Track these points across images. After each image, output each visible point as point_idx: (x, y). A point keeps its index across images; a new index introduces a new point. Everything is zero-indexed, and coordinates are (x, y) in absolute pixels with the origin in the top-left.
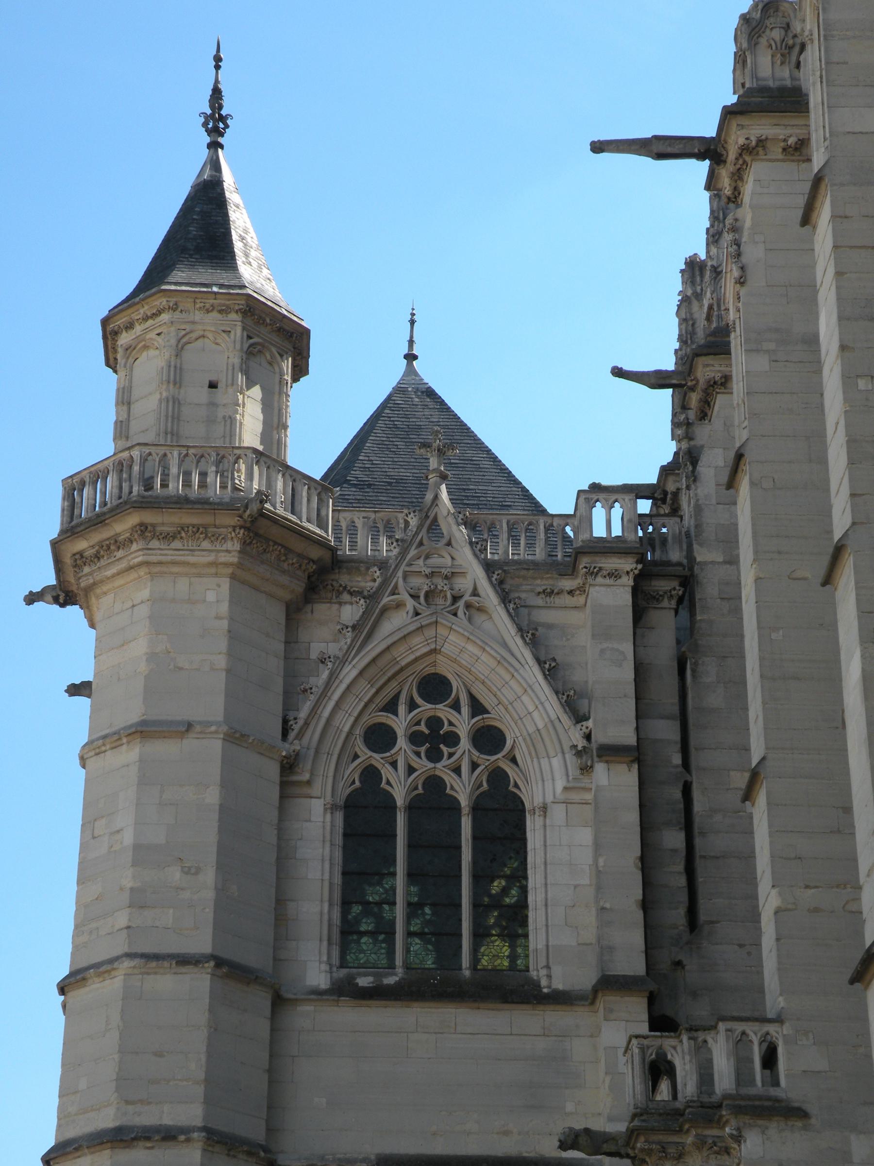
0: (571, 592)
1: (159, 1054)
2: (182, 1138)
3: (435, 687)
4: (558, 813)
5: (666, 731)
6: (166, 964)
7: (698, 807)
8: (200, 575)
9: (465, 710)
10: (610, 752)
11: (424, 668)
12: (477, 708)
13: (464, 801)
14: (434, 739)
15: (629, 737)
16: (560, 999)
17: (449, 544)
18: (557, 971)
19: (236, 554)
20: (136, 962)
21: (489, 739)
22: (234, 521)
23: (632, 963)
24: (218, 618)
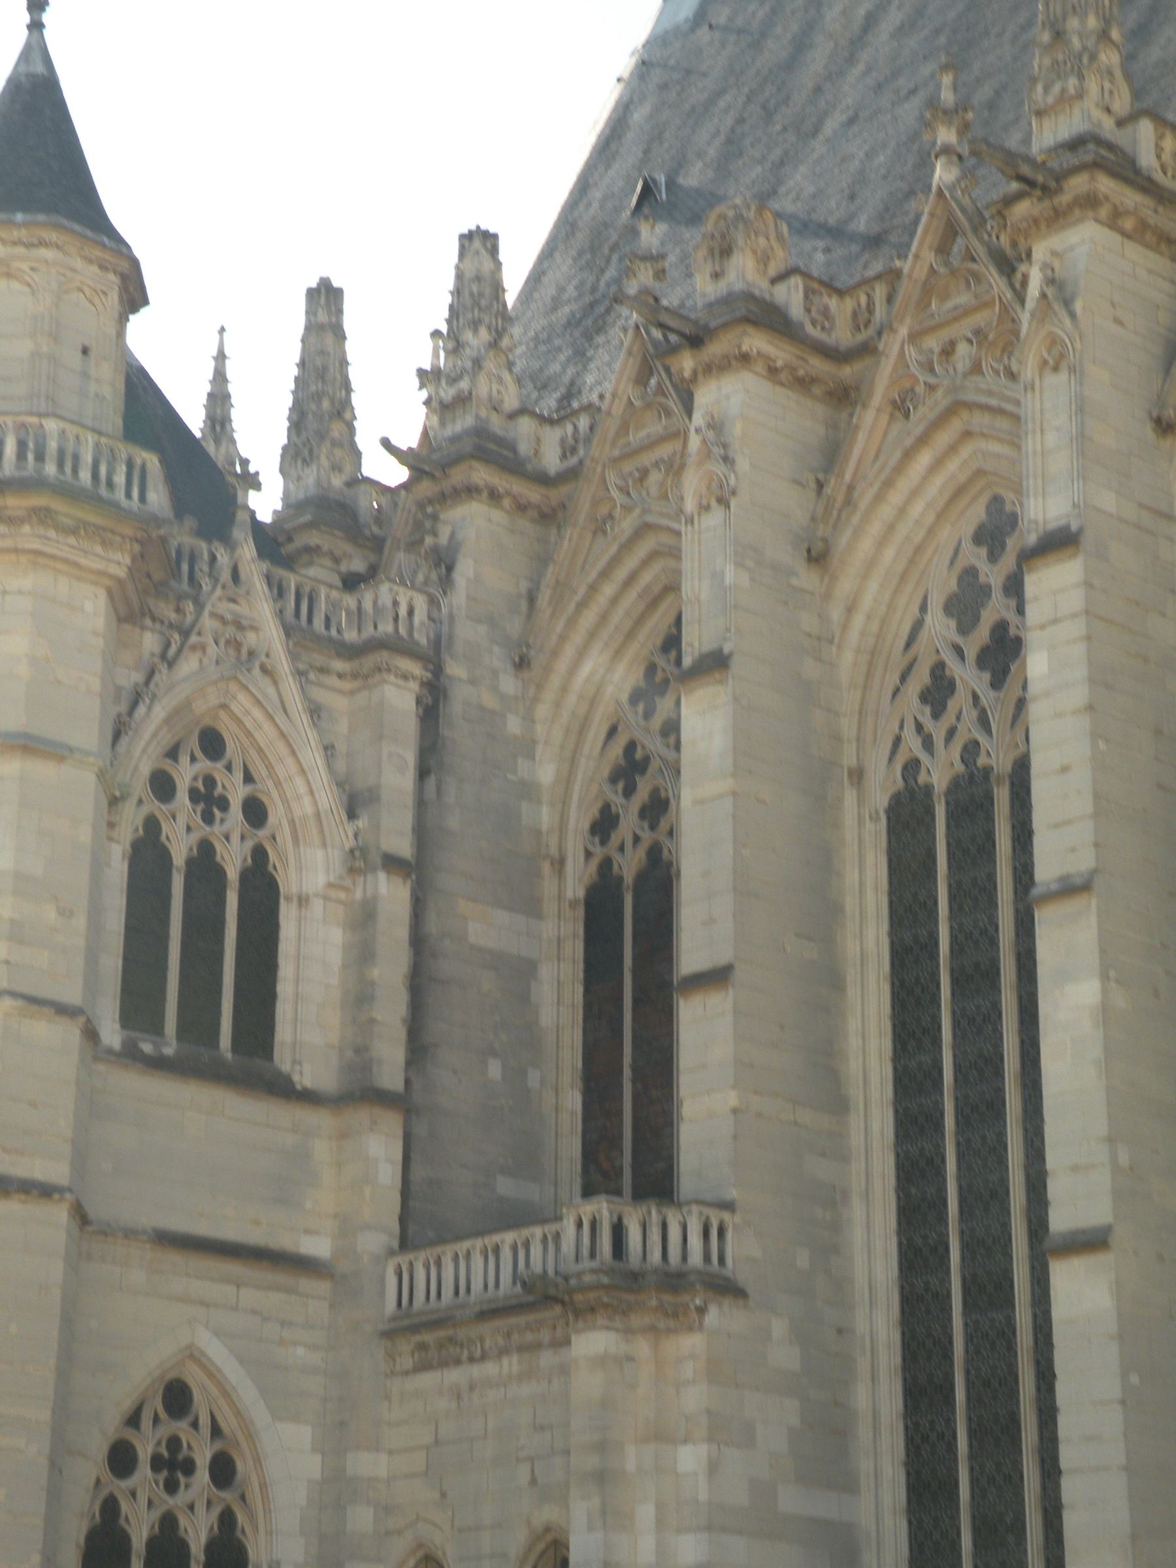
0: (340, 676)
1: (33, 1105)
2: (56, 1196)
3: (212, 744)
4: (317, 906)
6: (46, 1010)
8: (79, 579)
9: (239, 776)
11: (207, 721)
12: (248, 778)
13: (233, 874)
14: (209, 800)
16: (309, 1097)
17: (248, 593)
18: (307, 1068)
19: (125, 569)
20: (20, 1003)
21: (255, 812)
22: (129, 531)
23: (391, 1077)
24: (95, 633)
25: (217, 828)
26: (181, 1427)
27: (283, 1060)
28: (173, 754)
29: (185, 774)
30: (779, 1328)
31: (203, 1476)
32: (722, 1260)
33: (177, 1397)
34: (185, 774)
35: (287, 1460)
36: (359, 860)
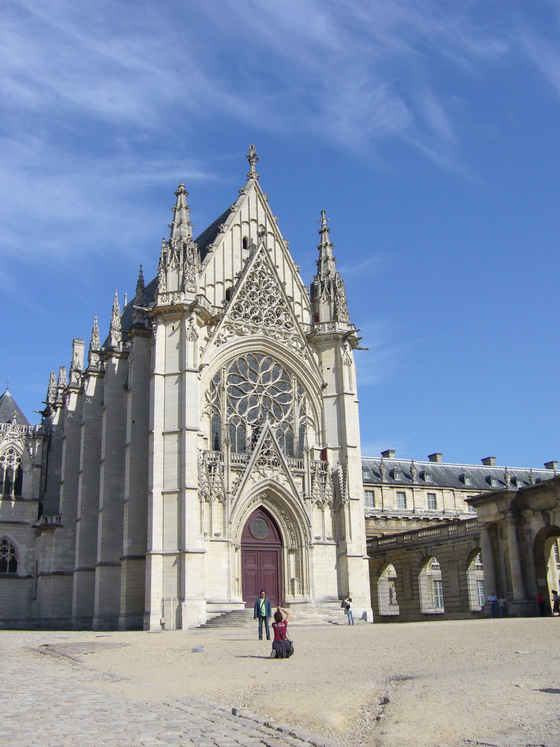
4: (28, 473)
5: (45, 461)
7: (48, 473)
10: (38, 466)
15: (40, 464)
16: (26, 500)
23: (37, 497)
25: (11, 464)
26: (5, 546)
27: (23, 495)
28: (4, 454)
29: (6, 457)
30: (69, 530)
31: (9, 552)
32: (60, 522)
33: (5, 542)
34: (6, 457)
35: (22, 550)
36: (33, 466)
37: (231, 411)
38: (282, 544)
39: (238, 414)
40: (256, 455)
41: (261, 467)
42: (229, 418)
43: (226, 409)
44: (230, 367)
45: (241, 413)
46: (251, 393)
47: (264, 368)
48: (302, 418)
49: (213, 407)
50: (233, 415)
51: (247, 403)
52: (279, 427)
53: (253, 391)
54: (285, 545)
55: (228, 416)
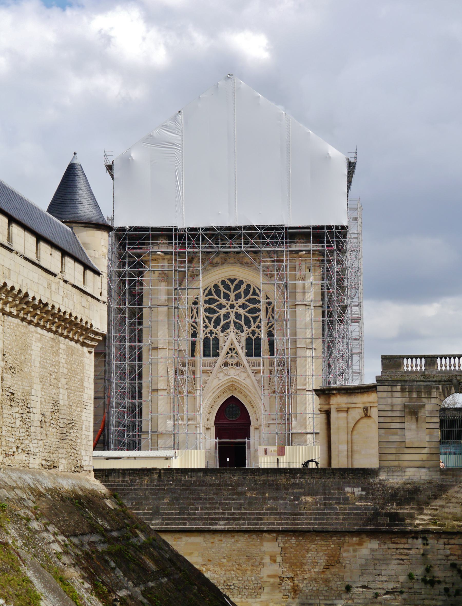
37: (206, 327)
38: (250, 423)
39: (212, 328)
40: (220, 360)
41: (225, 368)
42: (205, 332)
43: (202, 325)
44: (207, 292)
45: (215, 327)
46: (223, 312)
47: (235, 289)
48: (270, 324)
49: (192, 326)
50: (208, 329)
51: (220, 319)
52: (248, 334)
53: (226, 308)
54: (252, 424)
55: (204, 331)
